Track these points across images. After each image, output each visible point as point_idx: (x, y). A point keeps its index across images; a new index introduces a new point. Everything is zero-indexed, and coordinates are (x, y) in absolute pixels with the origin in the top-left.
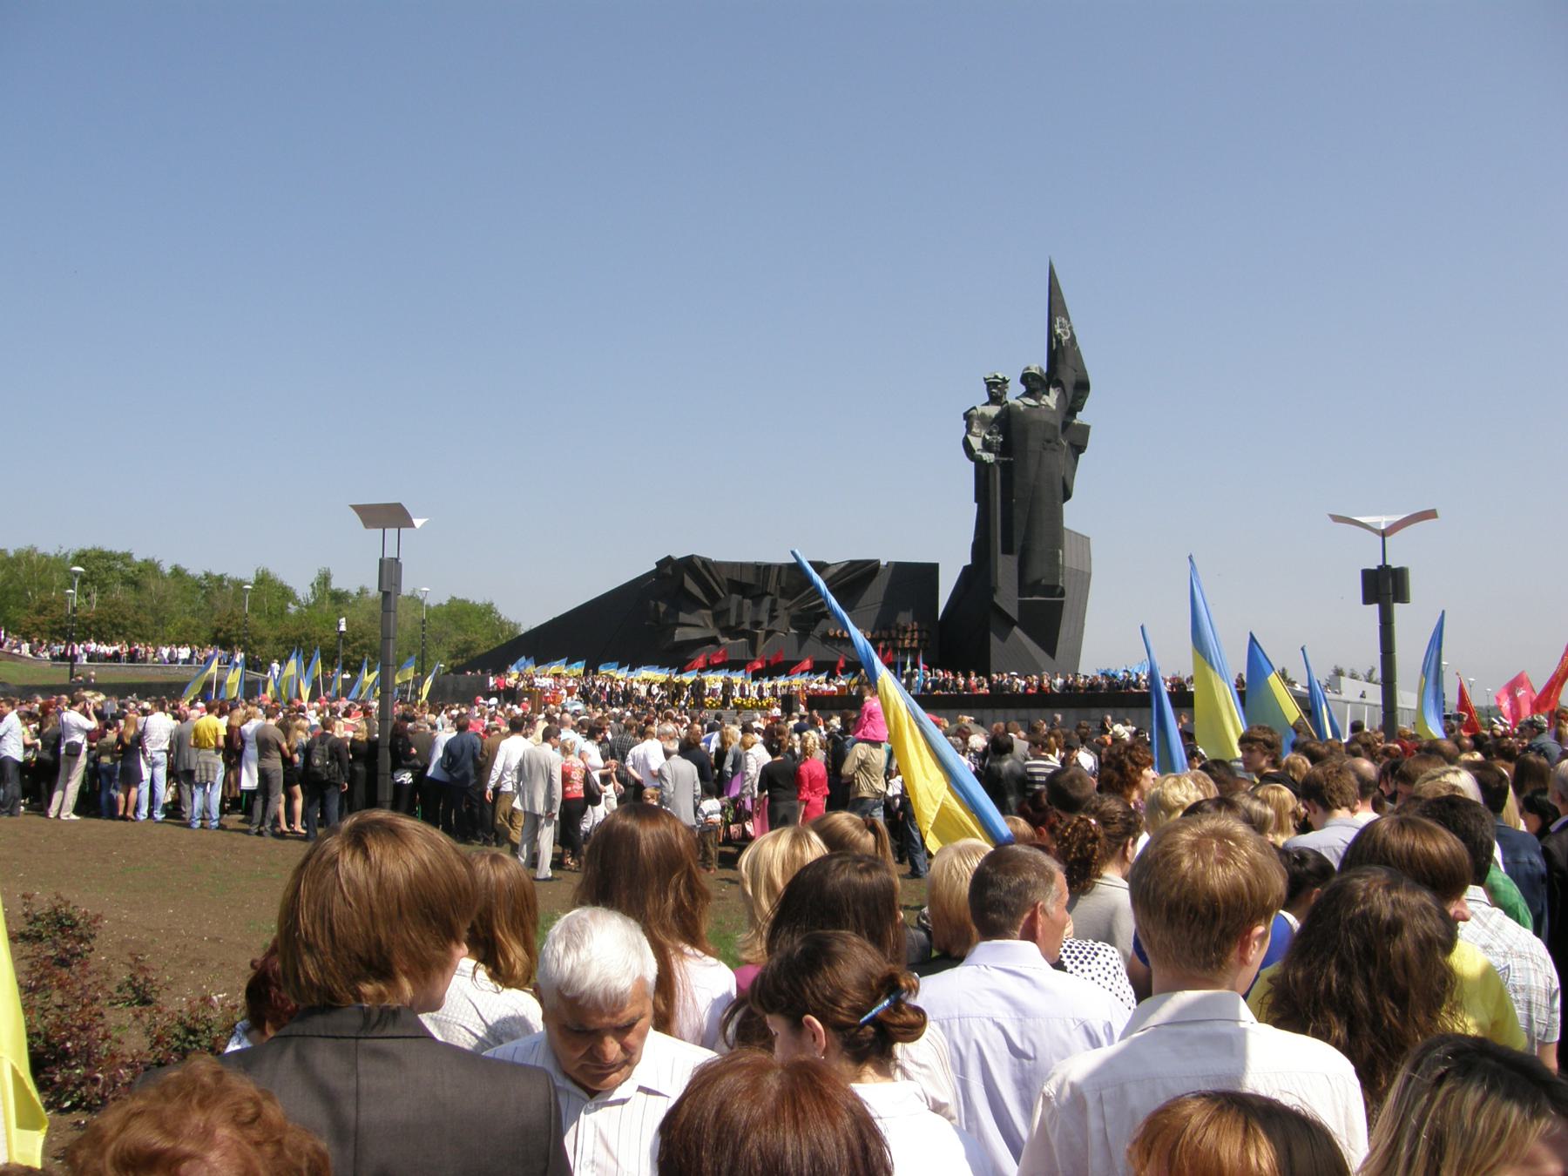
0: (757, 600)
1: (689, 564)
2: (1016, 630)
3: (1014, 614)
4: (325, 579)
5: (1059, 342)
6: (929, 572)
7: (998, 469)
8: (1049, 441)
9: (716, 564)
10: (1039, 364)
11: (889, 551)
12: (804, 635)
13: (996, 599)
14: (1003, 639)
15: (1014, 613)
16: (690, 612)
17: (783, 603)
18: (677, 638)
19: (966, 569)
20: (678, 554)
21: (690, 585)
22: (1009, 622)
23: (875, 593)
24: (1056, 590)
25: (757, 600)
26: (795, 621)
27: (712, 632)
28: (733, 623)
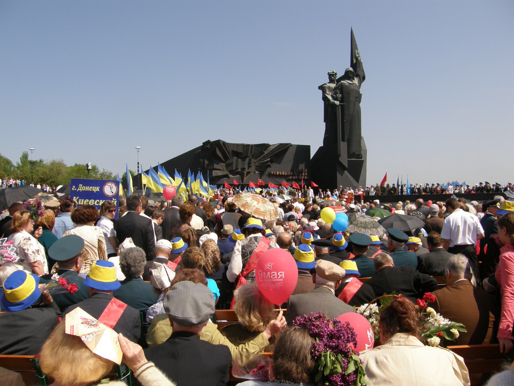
0: (244, 159)
1: (218, 143)
2: (346, 171)
3: (347, 166)
4: (25, 157)
6: (306, 149)
8: (357, 98)
9: (227, 143)
11: (296, 140)
12: (261, 174)
13: (340, 160)
14: (342, 174)
15: (346, 164)
16: (217, 164)
17: (253, 160)
19: (321, 148)
20: (213, 139)
22: (343, 168)
23: (289, 156)
24: (359, 156)
25: (244, 159)
26: (258, 168)
27: (226, 173)
28: (234, 169)
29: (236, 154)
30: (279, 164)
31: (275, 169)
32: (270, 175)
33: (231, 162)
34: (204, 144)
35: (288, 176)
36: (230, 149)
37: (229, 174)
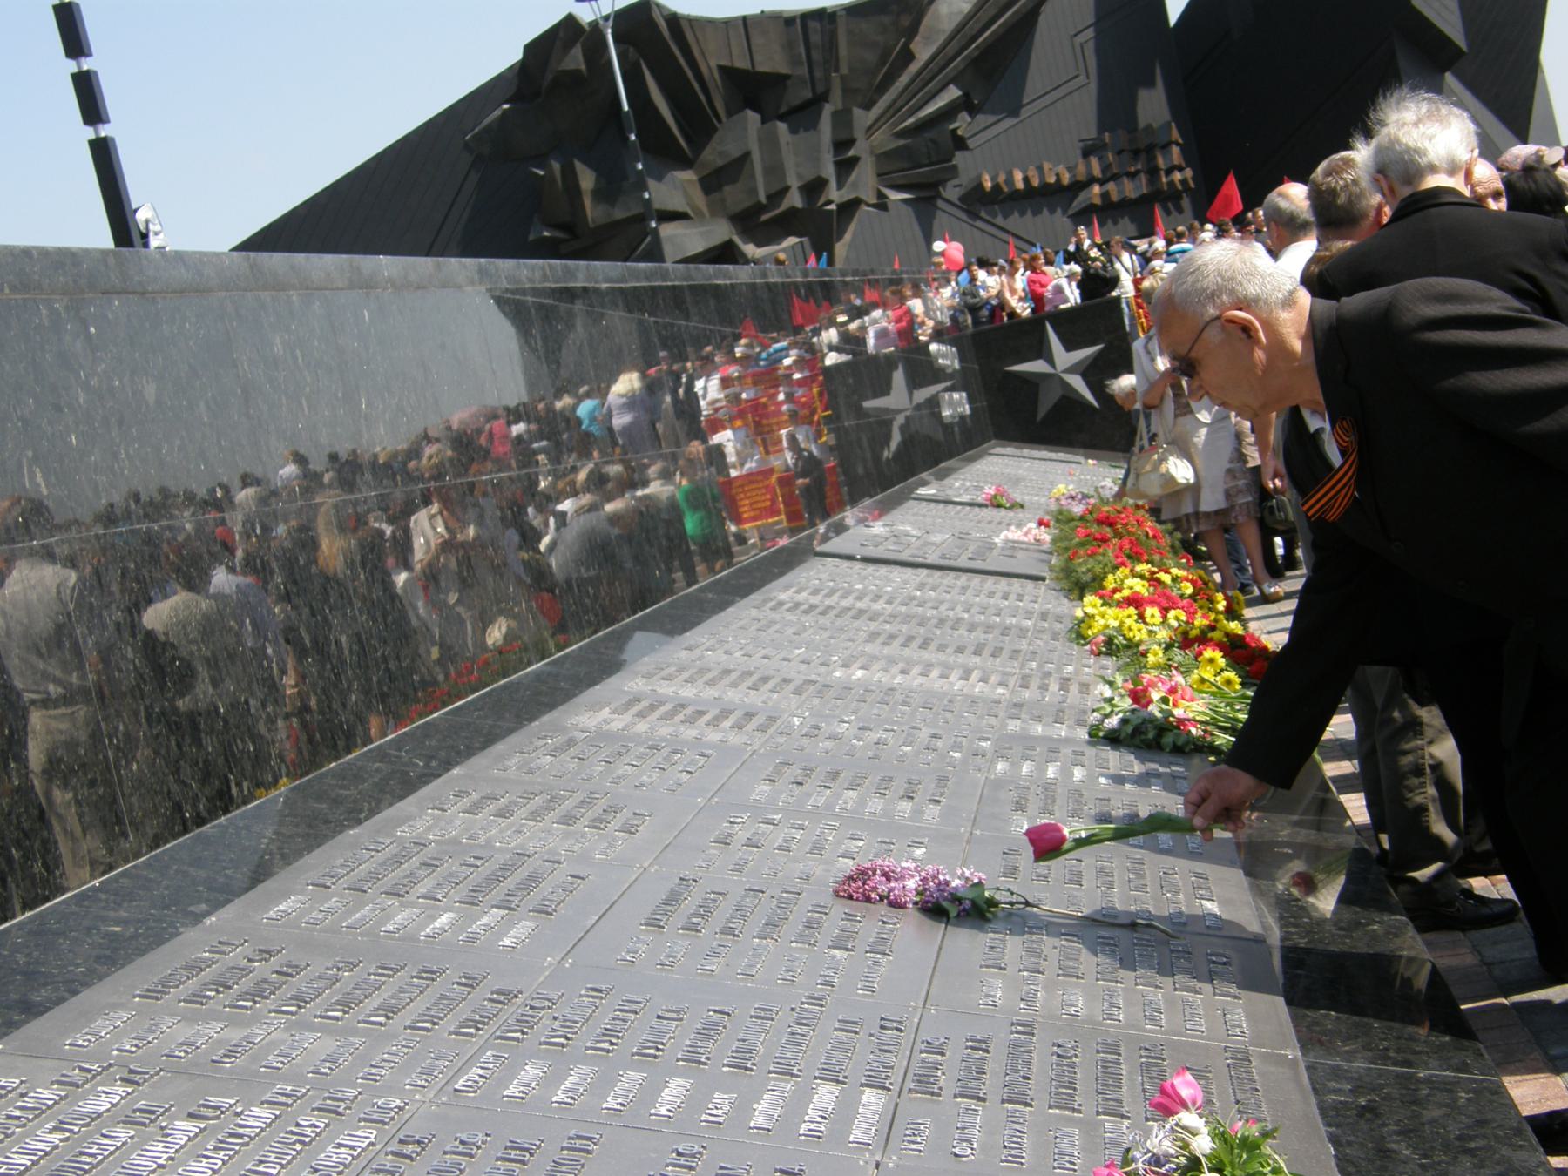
0: (803, 115)
9: (694, 22)
12: (925, 197)
26: (893, 168)
27: (721, 231)
29: (752, 90)
30: (1014, 112)
31: (995, 153)
32: (979, 202)
33: (735, 152)
34: (540, 50)
35: (1078, 186)
36: (712, 59)
37: (737, 240)
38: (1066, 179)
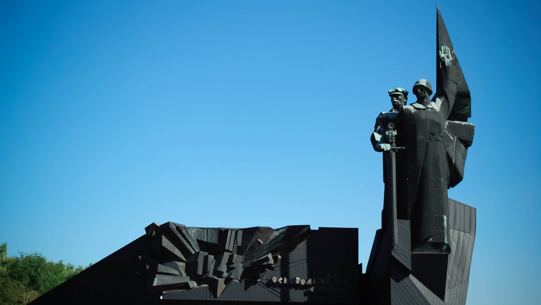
3: (409, 266)
5: (444, 63)
6: (351, 236)
7: (394, 154)
9: (185, 228)
10: (428, 79)
13: (393, 254)
18: (155, 284)
19: (378, 232)
21: (166, 243)
38: (303, 283)
